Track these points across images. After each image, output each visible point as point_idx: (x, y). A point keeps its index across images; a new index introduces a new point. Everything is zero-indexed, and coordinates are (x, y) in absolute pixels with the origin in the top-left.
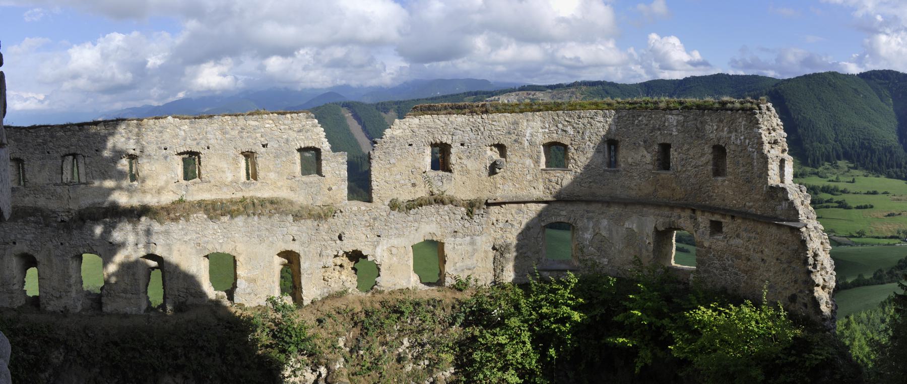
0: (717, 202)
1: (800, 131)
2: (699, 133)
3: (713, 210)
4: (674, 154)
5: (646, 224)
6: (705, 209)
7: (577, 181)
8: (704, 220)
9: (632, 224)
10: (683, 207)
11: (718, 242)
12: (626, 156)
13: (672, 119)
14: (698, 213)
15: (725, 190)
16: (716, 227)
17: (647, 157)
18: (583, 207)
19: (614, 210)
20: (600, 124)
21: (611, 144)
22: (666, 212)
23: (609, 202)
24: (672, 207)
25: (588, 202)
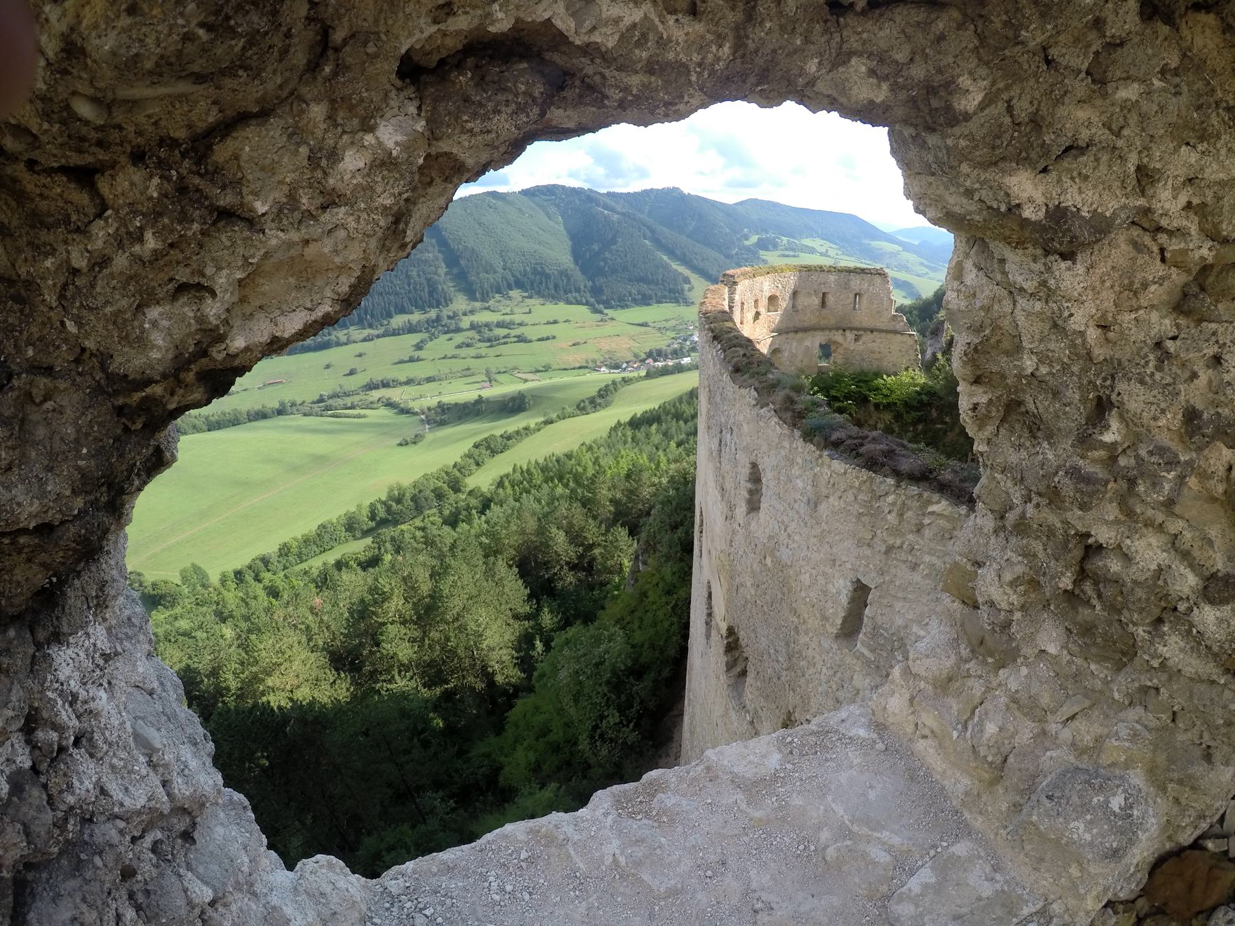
0: (856, 324)
1: (463, 262)
2: (847, 286)
3: (858, 329)
4: (831, 299)
5: (814, 342)
6: (851, 329)
7: (781, 322)
8: (850, 336)
9: (808, 343)
10: (837, 329)
11: (859, 346)
12: (803, 301)
13: (832, 278)
14: (848, 333)
15: (863, 317)
16: (857, 339)
17: (816, 301)
18: (784, 336)
19: (800, 335)
20: (792, 280)
21: (795, 294)
22: (827, 333)
23: (796, 332)
24: (830, 330)
25: (787, 333)
